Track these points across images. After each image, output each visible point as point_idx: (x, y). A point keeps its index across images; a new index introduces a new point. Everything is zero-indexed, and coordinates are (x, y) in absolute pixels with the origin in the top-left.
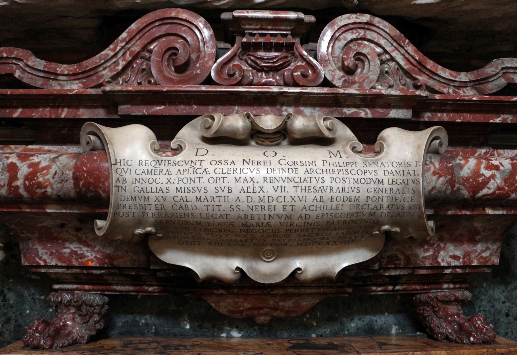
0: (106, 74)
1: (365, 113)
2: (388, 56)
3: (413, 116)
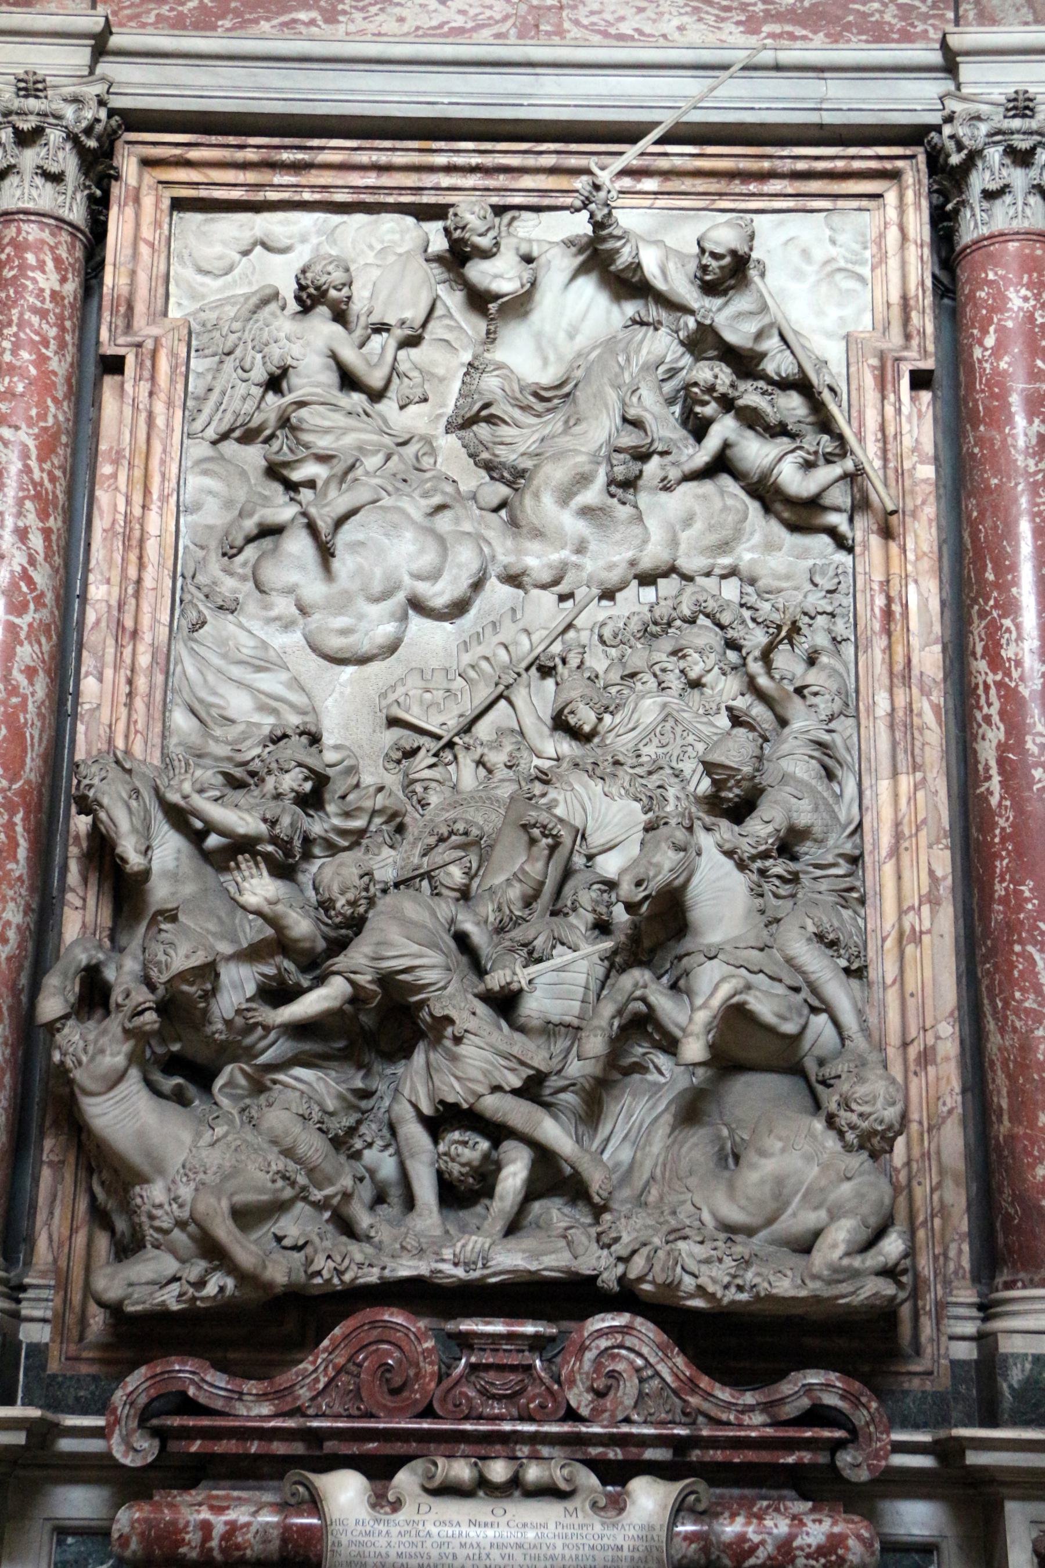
0: (304, 1394)
1: (615, 1454)
2: (650, 1372)
3: (675, 1454)
